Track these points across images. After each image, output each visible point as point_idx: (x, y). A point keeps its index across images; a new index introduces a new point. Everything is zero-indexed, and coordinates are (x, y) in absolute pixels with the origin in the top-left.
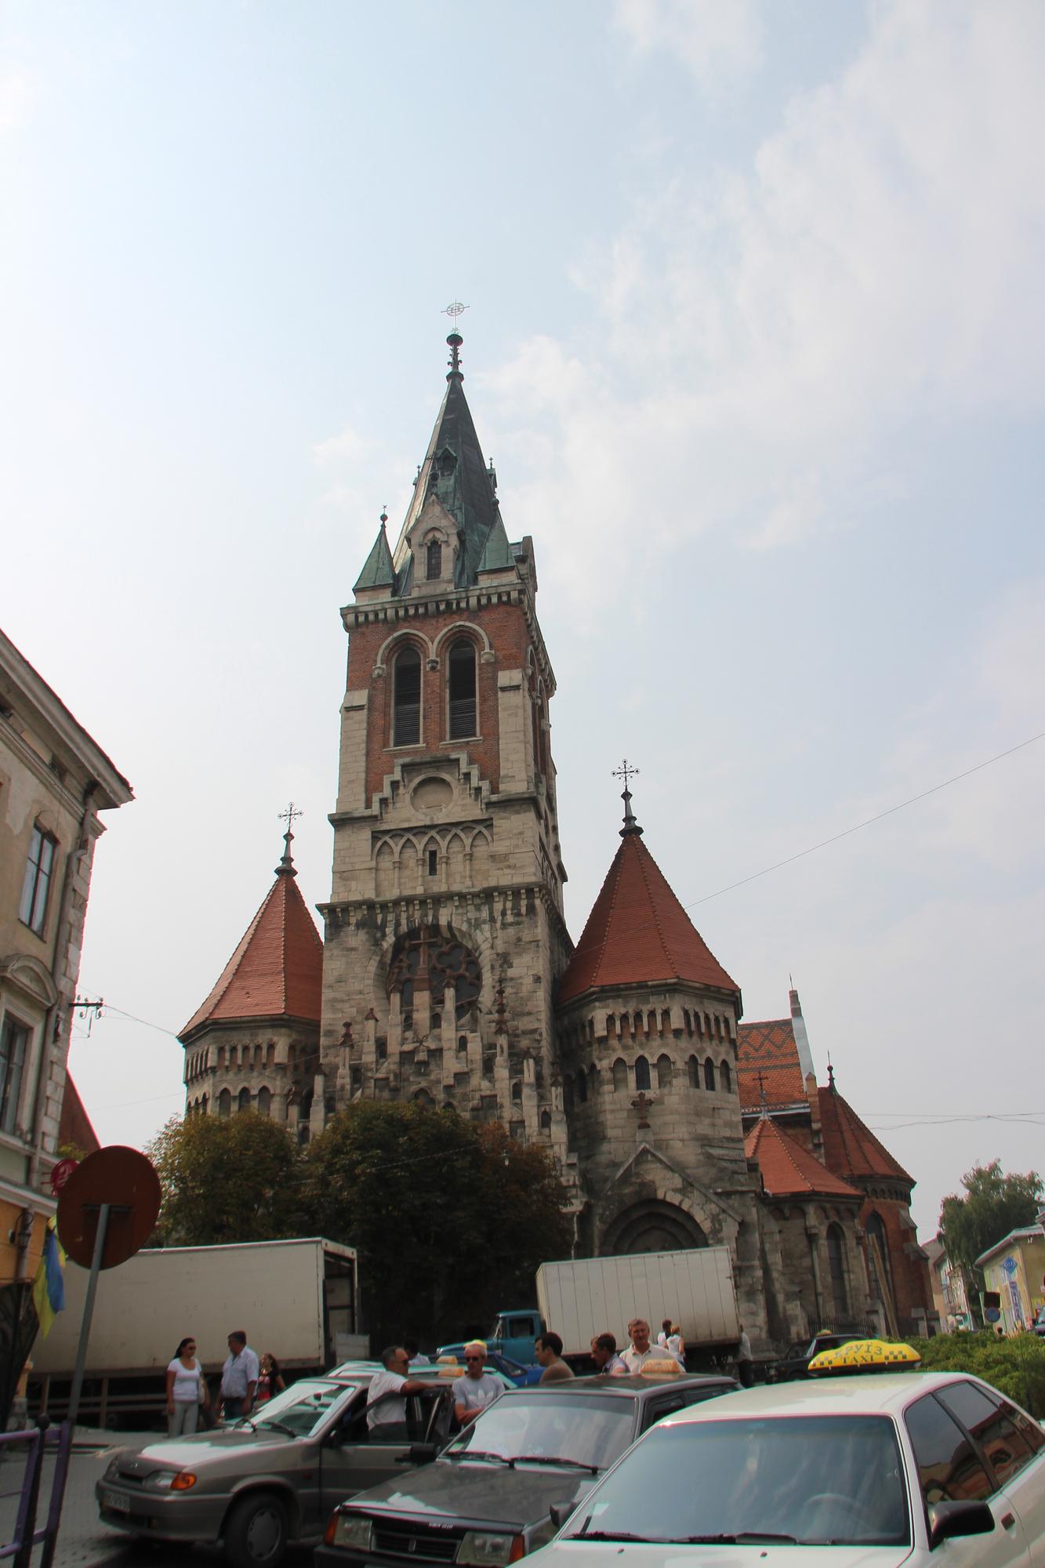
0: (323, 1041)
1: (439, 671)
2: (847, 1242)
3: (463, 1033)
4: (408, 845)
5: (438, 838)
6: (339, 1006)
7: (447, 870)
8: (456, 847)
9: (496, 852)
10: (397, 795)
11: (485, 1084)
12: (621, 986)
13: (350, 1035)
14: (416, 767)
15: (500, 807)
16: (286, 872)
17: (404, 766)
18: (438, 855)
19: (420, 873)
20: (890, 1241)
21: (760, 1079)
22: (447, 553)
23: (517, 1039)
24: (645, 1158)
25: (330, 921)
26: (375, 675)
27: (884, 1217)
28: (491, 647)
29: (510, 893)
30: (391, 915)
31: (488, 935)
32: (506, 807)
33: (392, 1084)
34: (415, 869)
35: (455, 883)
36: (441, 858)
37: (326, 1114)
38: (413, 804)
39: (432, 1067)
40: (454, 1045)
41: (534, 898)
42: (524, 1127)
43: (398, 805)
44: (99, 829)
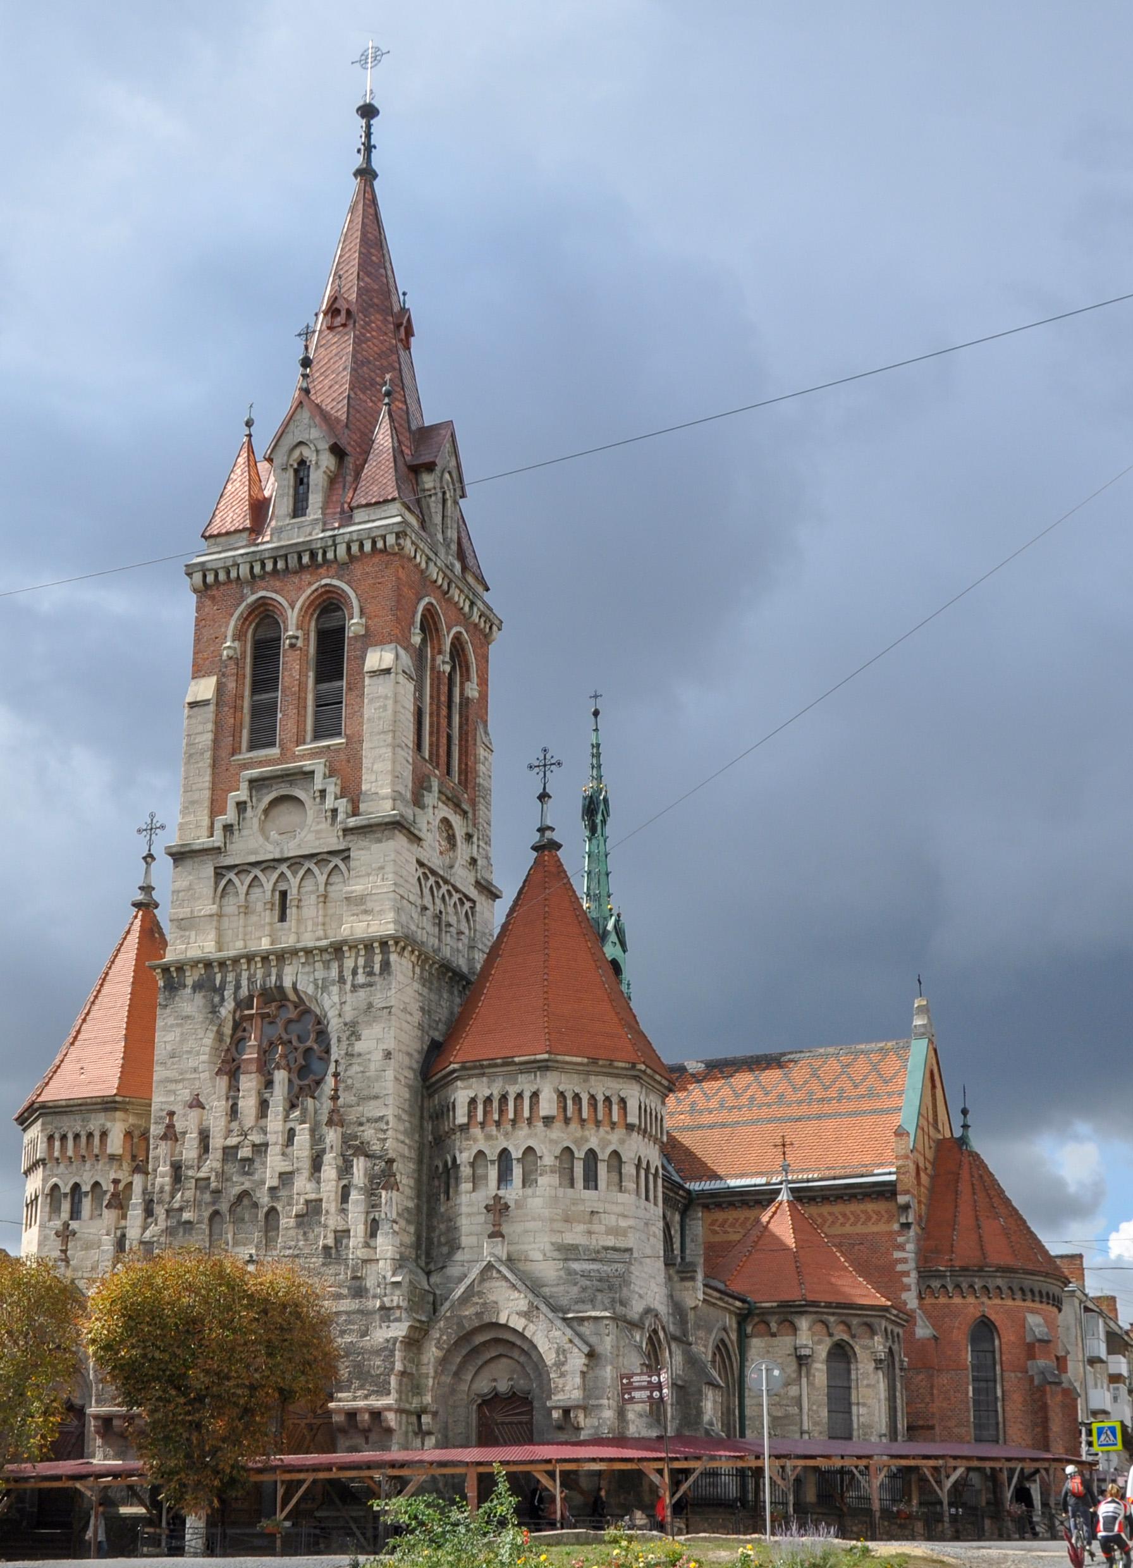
1: (301, 649)
2: (860, 1366)
3: (291, 1125)
4: (256, 883)
5: (288, 874)
6: (173, 1086)
7: (298, 914)
8: (309, 885)
9: (352, 892)
10: (244, 819)
11: (310, 1186)
12: (485, 1063)
13: (173, 1126)
14: (266, 782)
15: (360, 834)
17: (252, 782)
18: (289, 898)
19: (267, 920)
20: (1004, 1358)
21: (784, 1145)
23: (362, 1128)
24: (489, 1274)
25: (164, 982)
26: (224, 658)
27: (997, 1324)
29: (361, 946)
30: (231, 974)
31: (336, 999)
32: (365, 833)
33: (213, 1185)
34: (263, 913)
35: (306, 932)
36: (291, 900)
37: (146, 1218)
38: (262, 830)
39: (257, 1165)
40: (281, 1140)
41: (389, 952)
42: (349, 1237)
43: (245, 832)
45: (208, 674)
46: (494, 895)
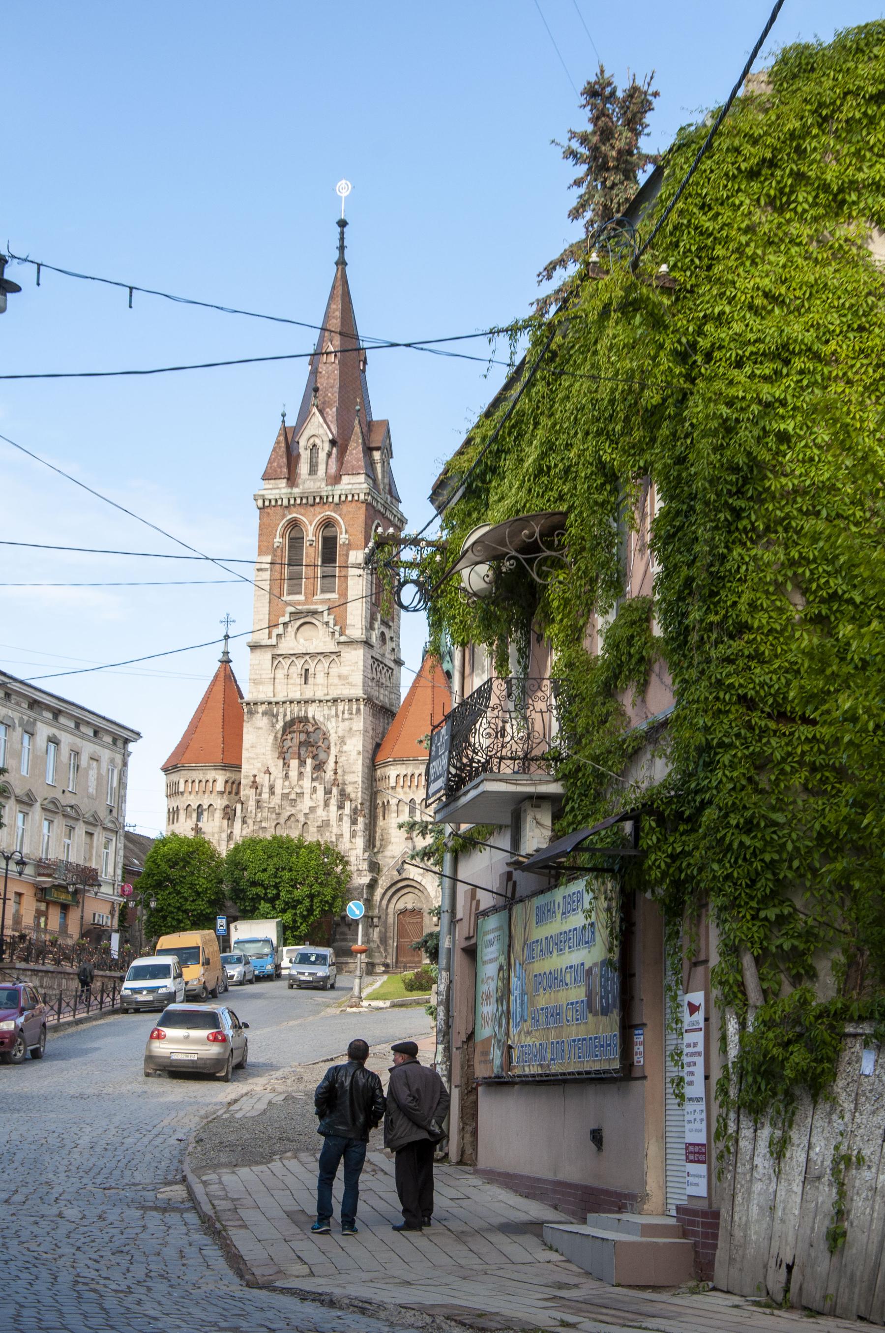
0: (243, 781)
6: (252, 761)
8: (319, 666)
11: (324, 814)
16: (226, 662)
22: (322, 456)
28: (346, 532)
40: (309, 791)
44: (130, 754)
45: (266, 554)
46: (399, 663)
